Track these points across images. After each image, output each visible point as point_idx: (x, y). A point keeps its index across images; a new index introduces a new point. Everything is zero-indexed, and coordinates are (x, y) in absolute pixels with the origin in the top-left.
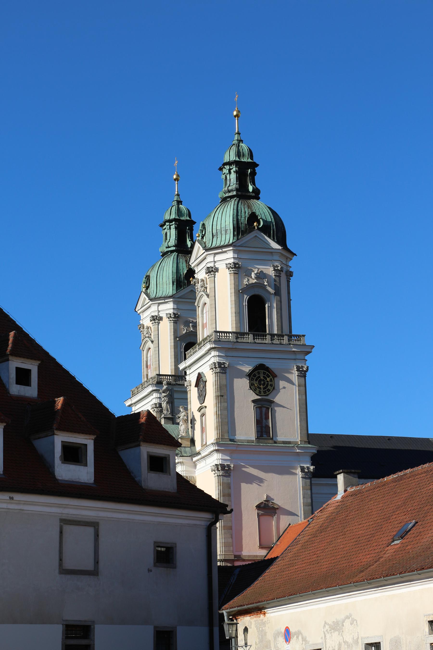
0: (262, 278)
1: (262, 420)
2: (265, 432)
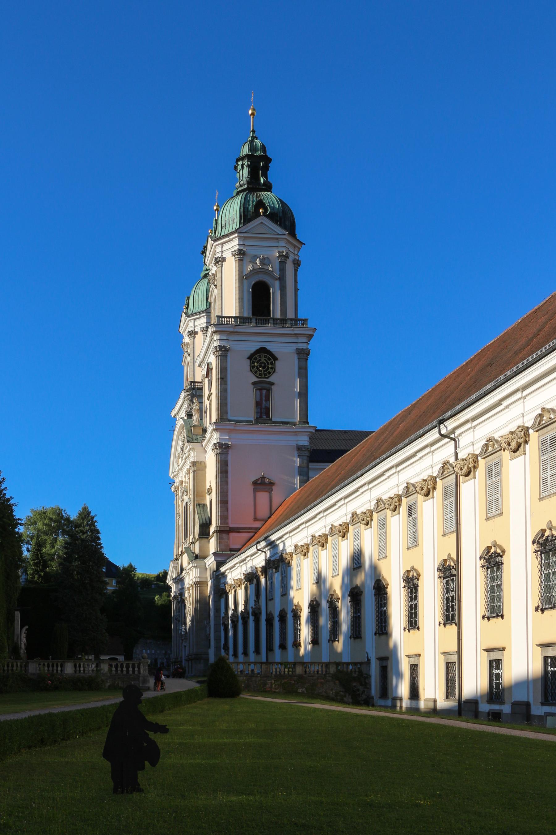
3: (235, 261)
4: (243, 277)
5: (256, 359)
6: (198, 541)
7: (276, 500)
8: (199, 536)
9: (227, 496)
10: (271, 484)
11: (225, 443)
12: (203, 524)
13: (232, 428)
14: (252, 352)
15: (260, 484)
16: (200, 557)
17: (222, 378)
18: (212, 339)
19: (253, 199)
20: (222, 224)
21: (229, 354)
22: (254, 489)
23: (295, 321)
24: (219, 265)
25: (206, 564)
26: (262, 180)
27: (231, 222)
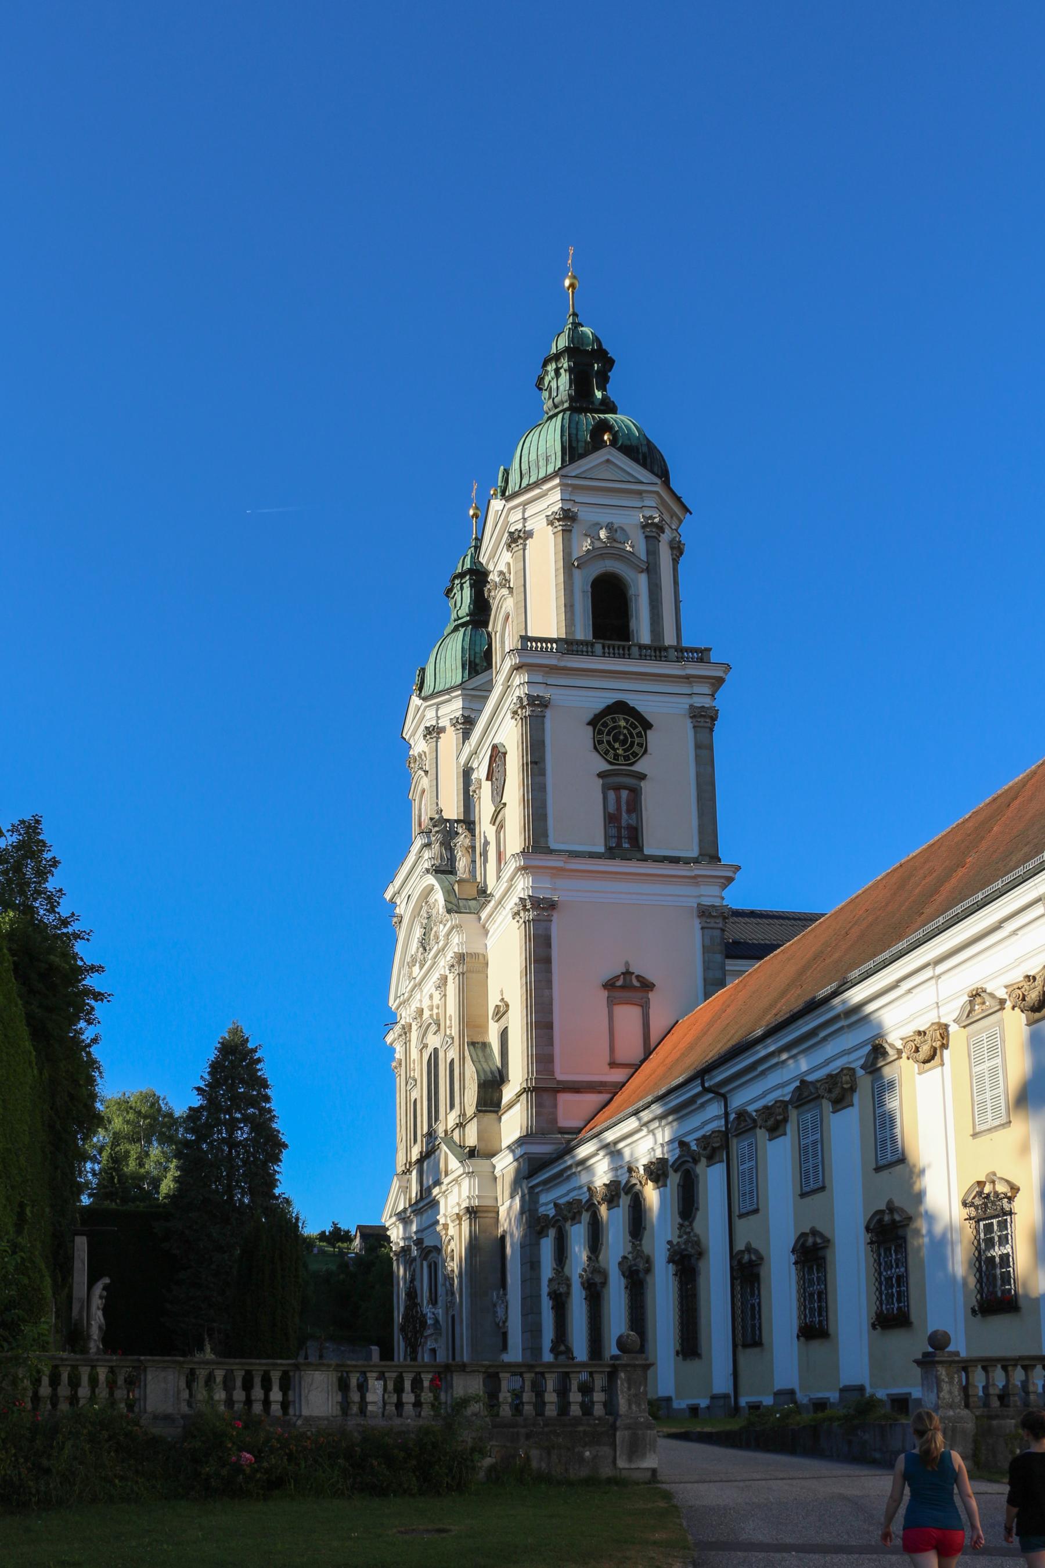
0: (620, 542)
1: (621, 814)
2: (626, 838)
3: (554, 534)
4: (573, 564)
5: (605, 725)
6: (475, 1119)
7: (658, 1024)
8: (477, 1107)
10: (647, 986)
11: (544, 898)
12: (485, 1081)
14: (597, 711)
15: (623, 987)
16: (481, 1152)
18: (509, 686)
19: (588, 420)
20: (522, 469)
21: (548, 713)
22: (608, 997)
23: (681, 653)
24: (518, 546)
25: (494, 1167)
26: (599, 394)
27: (542, 463)
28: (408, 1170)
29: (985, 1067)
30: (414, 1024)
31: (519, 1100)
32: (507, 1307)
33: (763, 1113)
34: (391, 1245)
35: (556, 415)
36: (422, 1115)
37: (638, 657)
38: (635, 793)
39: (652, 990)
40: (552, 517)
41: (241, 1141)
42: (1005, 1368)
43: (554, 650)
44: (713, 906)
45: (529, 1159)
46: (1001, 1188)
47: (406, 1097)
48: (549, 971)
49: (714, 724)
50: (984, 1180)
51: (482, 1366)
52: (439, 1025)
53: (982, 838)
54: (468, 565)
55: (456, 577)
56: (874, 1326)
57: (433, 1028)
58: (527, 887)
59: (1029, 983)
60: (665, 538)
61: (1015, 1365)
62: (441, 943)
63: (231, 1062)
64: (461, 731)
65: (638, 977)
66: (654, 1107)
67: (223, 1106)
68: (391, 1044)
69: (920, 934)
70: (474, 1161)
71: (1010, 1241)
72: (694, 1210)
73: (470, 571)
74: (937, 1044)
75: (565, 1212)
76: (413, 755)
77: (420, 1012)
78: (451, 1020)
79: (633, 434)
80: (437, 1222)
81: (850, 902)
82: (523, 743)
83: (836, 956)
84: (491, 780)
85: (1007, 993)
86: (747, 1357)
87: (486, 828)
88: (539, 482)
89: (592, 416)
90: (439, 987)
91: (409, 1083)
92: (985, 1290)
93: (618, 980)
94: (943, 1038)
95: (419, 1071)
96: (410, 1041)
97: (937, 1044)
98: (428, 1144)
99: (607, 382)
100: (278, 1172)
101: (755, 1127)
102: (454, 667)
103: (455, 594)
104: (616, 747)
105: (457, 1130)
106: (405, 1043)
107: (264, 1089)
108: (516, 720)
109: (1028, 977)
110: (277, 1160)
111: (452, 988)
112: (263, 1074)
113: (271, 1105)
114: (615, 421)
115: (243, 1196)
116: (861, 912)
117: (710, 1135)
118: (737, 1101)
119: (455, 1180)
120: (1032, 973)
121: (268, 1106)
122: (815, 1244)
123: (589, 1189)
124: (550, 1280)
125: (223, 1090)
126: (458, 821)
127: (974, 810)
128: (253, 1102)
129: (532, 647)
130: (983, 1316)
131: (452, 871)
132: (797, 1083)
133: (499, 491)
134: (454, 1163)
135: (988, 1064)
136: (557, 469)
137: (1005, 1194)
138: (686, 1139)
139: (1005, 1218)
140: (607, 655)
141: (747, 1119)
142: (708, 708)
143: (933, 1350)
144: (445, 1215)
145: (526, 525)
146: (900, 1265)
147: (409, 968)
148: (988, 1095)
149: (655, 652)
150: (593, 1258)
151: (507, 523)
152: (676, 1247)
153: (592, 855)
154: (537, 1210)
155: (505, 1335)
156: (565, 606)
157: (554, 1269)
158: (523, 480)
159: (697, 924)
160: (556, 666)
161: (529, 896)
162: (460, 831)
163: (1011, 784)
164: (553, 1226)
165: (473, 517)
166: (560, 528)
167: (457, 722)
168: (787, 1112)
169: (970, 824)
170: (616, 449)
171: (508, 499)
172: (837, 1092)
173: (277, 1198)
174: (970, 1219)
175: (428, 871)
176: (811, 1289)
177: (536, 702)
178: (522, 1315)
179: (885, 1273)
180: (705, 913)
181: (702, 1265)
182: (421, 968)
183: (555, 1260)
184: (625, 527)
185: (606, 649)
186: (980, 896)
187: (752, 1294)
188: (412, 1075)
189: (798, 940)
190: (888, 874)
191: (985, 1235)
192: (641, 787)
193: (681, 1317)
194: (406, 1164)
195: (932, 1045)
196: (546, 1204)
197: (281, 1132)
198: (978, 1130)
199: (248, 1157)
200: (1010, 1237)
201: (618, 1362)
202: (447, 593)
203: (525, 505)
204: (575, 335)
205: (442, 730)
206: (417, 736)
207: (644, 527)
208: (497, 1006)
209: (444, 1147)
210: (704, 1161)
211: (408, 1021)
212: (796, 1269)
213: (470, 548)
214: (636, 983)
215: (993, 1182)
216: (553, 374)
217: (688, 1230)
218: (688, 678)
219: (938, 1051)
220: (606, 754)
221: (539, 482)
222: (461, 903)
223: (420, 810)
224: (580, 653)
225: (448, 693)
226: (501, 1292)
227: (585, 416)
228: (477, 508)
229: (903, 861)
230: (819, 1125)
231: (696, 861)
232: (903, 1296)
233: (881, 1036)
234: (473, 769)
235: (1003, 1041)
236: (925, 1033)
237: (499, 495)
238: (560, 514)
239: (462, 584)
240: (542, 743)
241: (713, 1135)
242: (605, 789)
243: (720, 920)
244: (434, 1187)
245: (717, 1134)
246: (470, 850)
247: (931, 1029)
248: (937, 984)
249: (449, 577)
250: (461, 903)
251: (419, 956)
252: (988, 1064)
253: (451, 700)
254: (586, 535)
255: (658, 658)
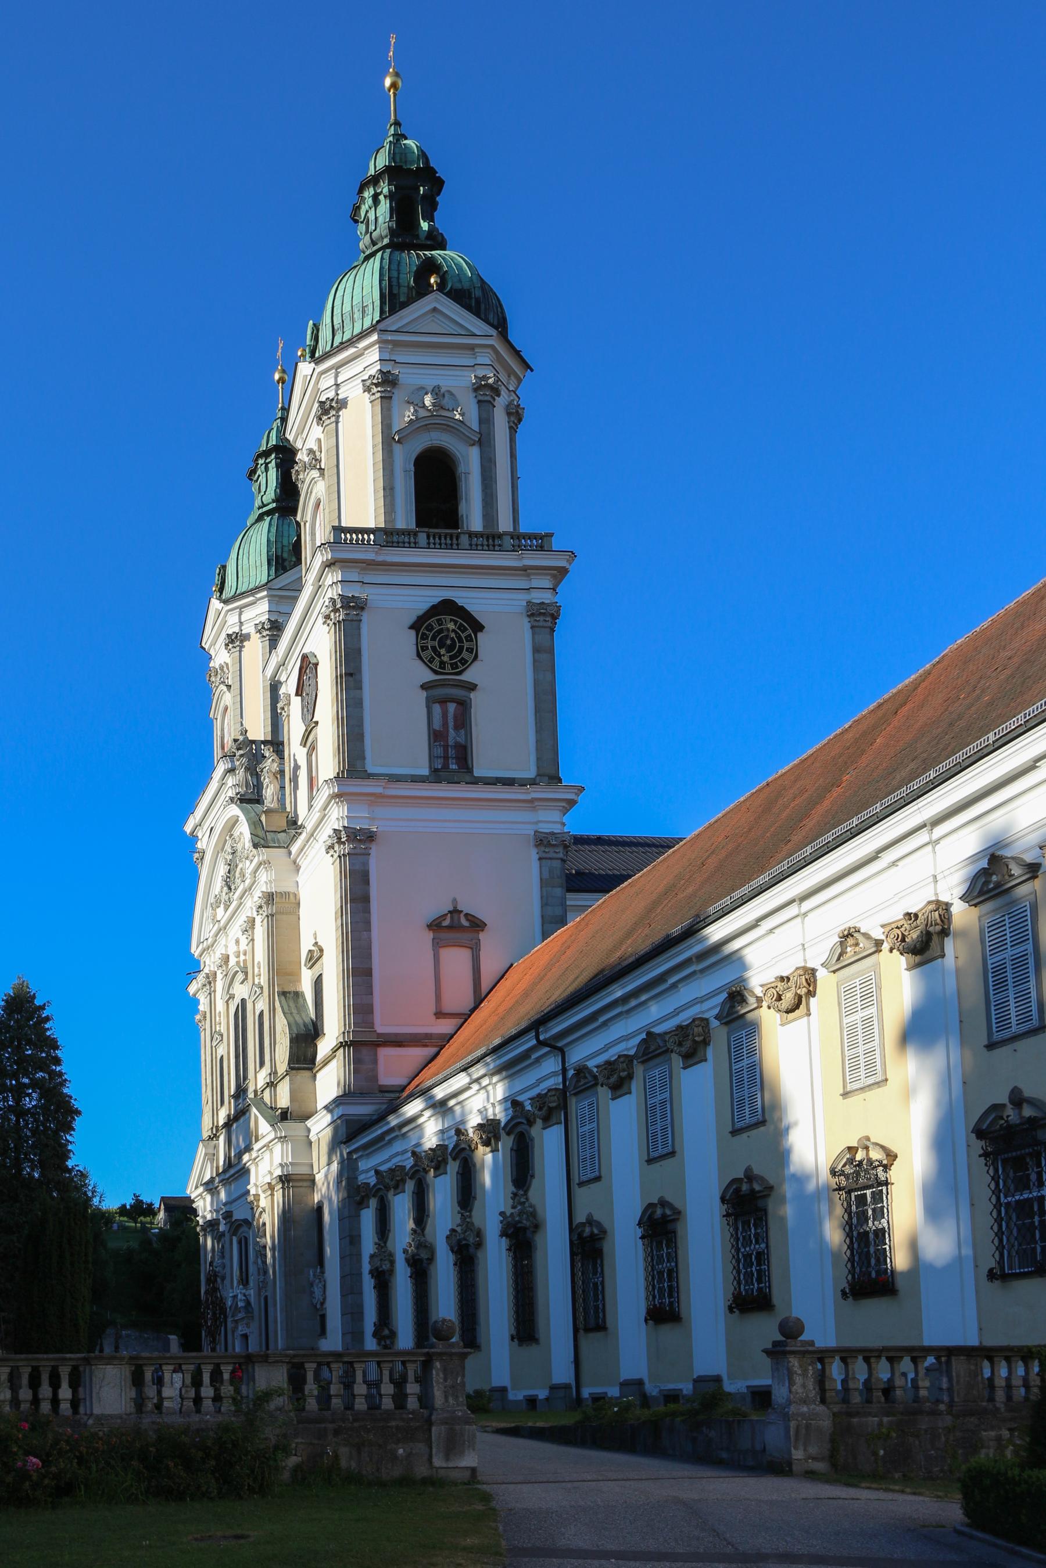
0: (448, 410)
1: (448, 731)
2: (453, 758)
3: (371, 402)
4: (393, 438)
6: (288, 1078)
7: (489, 969)
8: (289, 1064)
9: (369, 956)
10: (477, 925)
11: (361, 829)
12: (297, 1035)
13: (379, 790)
14: (421, 613)
15: (450, 927)
16: (294, 1114)
17: (349, 674)
18: (320, 586)
19: (412, 259)
20: (335, 324)
21: (365, 616)
22: (433, 939)
23: (519, 540)
24: (329, 418)
25: (309, 1130)
26: (425, 226)
27: (357, 315)
28: (215, 1135)
29: (857, 1017)
30: (219, 973)
31: (335, 1056)
32: (325, 1286)
33: (605, 1069)
34: (198, 1218)
35: (373, 254)
36: (229, 1074)
37: (468, 547)
38: (464, 706)
39: (483, 930)
40: (370, 381)
41: (29, 1109)
42: (867, 1360)
43: (372, 543)
44: (552, 834)
45: (347, 1121)
46: (876, 1155)
47: (212, 1054)
48: (367, 911)
49: (556, 623)
50: (857, 1146)
51: (287, 1356)
52: (246, 974)
53: (863, 752)
54: (273, 441)
55: (259, 456)
56: (731, 1309)
57: (240, 977)
58: (342, 817)
59: (909, 922)
60: (501, 402)
61: (879, 1357)
62: (248, 882)
63: (17, 1021)
64: (268, 638)
65: (467, 915)
66: (488, 1059)
67: (9, 1070)
68: (195, 995)
69: (784, 865)
70: (286, 1124)
71: (886, 1215)
72: (529, 1177)
73: (276, 449)
74: (803, 991)
75: (387, 1180)
76: (214, 668)
77: (226, 959)
78: (259, 968)
79: (465, 274)
80: (248, 1192)
81: (708, 828)
82: (336, 652)
83: (690, 890)
84: (301, 695)
85: (884, 933)
86: (590, 1343)
87: (296, 750)
88: (354, 339)
89: (417, 254)
90: (246, 931)
91: (215, 1038)
92: (857, 1270)
93: (444, 920)
94: (809, 985)
95: (225, 1025)
96: (215, 991)
97: (803, 991)
98: (236, 1106)
99: (435, 209)
100: (71, 1143)
101: (596, 1084)
102: (258, 563)
103: (259, 476)
104: (442, 653)
105: (268, 1090)
106: (210, 994)
107: (54, 1051)
108: (328, 625)
109: (908, 914)
110: (69, 1128)
111: (260, 932)
112: (53, 1034)
113: (61, 1068)
114: (444, 258)
115: (33, 1170)
116: (720, 839)
117: (546, 1094)
118: (577, 1054)
119: (266, 1146)
120: (913, 910)
121: (58, 1069)
122: (664, 1216)
123: (414, 1153)
124: (372, 1256)
125: (8, 1053)
126: (265, 742)
127: (856, 718)
128: (43, 1066)
129: (346, 539)
130: (854, 1299)
131: (259, 800)
132: (644, 1036)
133: (307, 351)
134: (264, 1127)
135: (861, 1014)
136: (374, 322)
137: (880, 1162)
138: (520, 1098)
139: (880, 1188)
140: (432, 546)
141: (587, 1075)
142: (548, 605)
143: (784, 1339)
144: (256, 1185)
145: (339, 392)
146: (760, 1241)
147: (213, 909)
148: (861, 1049)
149: (488, 541)
150: (419, 1231)
151: (317, 392)
152: (510, 1219)
153: (415, 779)
154: (357, 1178)
155: (323, 1317)
156: (384, 489)
157: (376, 1244)
158: (336, 337)
159: (534, 854)
160: (374, 560)
161: (344, 827)
162: (267, 754)
163: (900, 686)
164: (374, 1196)
165: (278, 382)
166: (379, 395)
167: (263, 628)
168: (632, 1068)
169: (849, 736)
170: (445, 294)
171: (318, 361)
172: (688, 1044)
173: (70, 1171)
174: (840, 1189)
175: (232, 799)
176: (660, 1266)
177: (351, 604)
178: (342, 1296)
179: (743, 1250)
180: (542, 841)
181: (538, 1239)
182: (226, 910)
183: (377, 1233)
184: (454, 391)
185: (431, 538)
186: (855, 821)
187: (595, 1273)
188: (218, 1029)
189: (648, 871)
190: (753, 794)
191: (857, 1208)
192: (471, 699)
193: (516, 1297)
194: (212, 1128)
195: (796, 993)
196: (367, 1171)
197: (74, 1098)
198: (849, 1089)
199: (38, 1126)
200: (885, 1210)
201: (433, 1350)
202: (250, 475)
203: (337, 367)
204: (397, 150)
205: (246, 637)
206: (217, 646)
207: (477, 388)
208: (310, 951)
209: (254, 1110)
210: (539, 1123)
211: (212, 969)
212: (643, 1245)
213: (275, 420)
214: (464, 922)
215: (867, 1148)
216: (370, 201)
217: (523, 1200)
218: (526, 570)
219: (804, 999)
220: (431, 662)
221: (354, 339)
222: (270, 836)
223: (222, 730)
224: (400, 545)
225: (253, 595)
226: (318, 1271)
227: (409, 253)
228: (284, 371)
229: (770, 779)
230: (669, 1082)
231: (533, 782)
232: (763, 1276)
233: (742, 981)
234: (281, 683)
235: (879, 988)
236: (788, 979)
237: (308, 356)
238: (378, 379)
239: (267, 464)
240: (359, 651)
241: (549, 1094)
242: (430, 702)
243: (560, 850)
244: (245, 1153)
245: (553, 1093)
246: (278, 776)
247: (796, 974)
248: (803, 923)
249: (253, 456)
250: (270, 836)
251: (224, 897)
252: (861, 1014)
253: (255, 603)
254: (408, 402)
255: (491, 547)
